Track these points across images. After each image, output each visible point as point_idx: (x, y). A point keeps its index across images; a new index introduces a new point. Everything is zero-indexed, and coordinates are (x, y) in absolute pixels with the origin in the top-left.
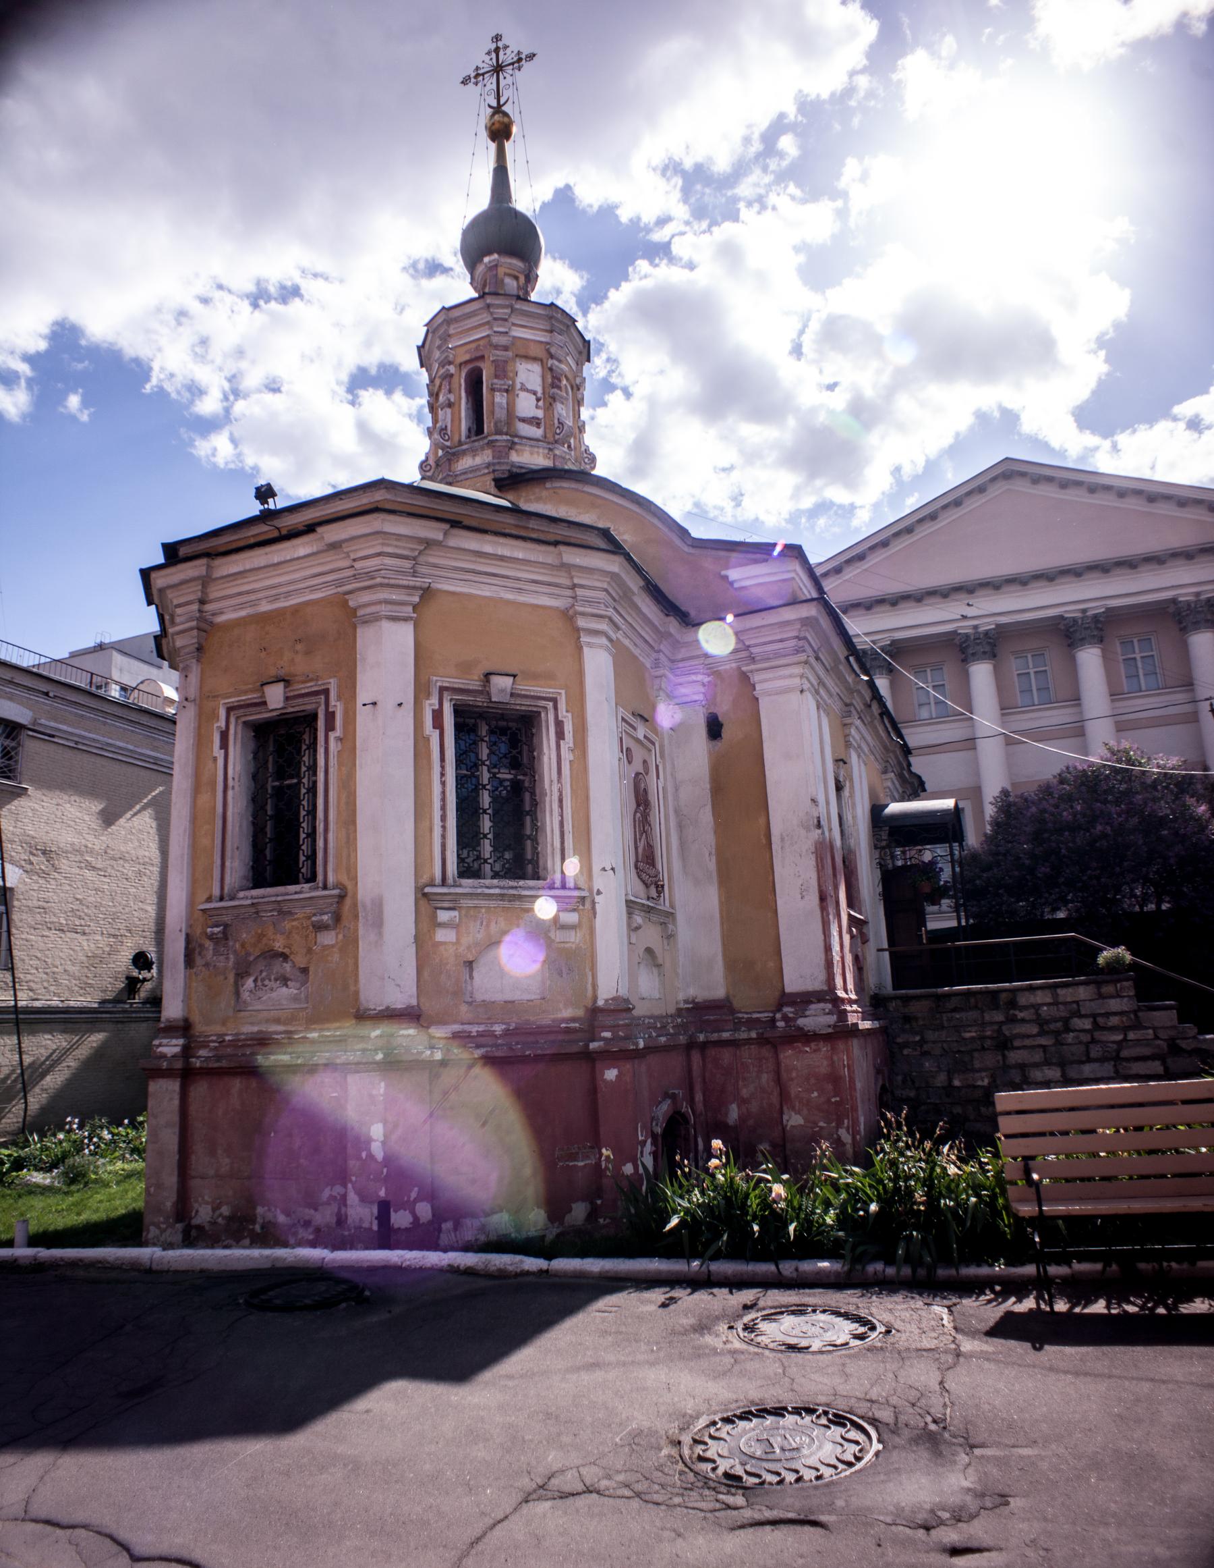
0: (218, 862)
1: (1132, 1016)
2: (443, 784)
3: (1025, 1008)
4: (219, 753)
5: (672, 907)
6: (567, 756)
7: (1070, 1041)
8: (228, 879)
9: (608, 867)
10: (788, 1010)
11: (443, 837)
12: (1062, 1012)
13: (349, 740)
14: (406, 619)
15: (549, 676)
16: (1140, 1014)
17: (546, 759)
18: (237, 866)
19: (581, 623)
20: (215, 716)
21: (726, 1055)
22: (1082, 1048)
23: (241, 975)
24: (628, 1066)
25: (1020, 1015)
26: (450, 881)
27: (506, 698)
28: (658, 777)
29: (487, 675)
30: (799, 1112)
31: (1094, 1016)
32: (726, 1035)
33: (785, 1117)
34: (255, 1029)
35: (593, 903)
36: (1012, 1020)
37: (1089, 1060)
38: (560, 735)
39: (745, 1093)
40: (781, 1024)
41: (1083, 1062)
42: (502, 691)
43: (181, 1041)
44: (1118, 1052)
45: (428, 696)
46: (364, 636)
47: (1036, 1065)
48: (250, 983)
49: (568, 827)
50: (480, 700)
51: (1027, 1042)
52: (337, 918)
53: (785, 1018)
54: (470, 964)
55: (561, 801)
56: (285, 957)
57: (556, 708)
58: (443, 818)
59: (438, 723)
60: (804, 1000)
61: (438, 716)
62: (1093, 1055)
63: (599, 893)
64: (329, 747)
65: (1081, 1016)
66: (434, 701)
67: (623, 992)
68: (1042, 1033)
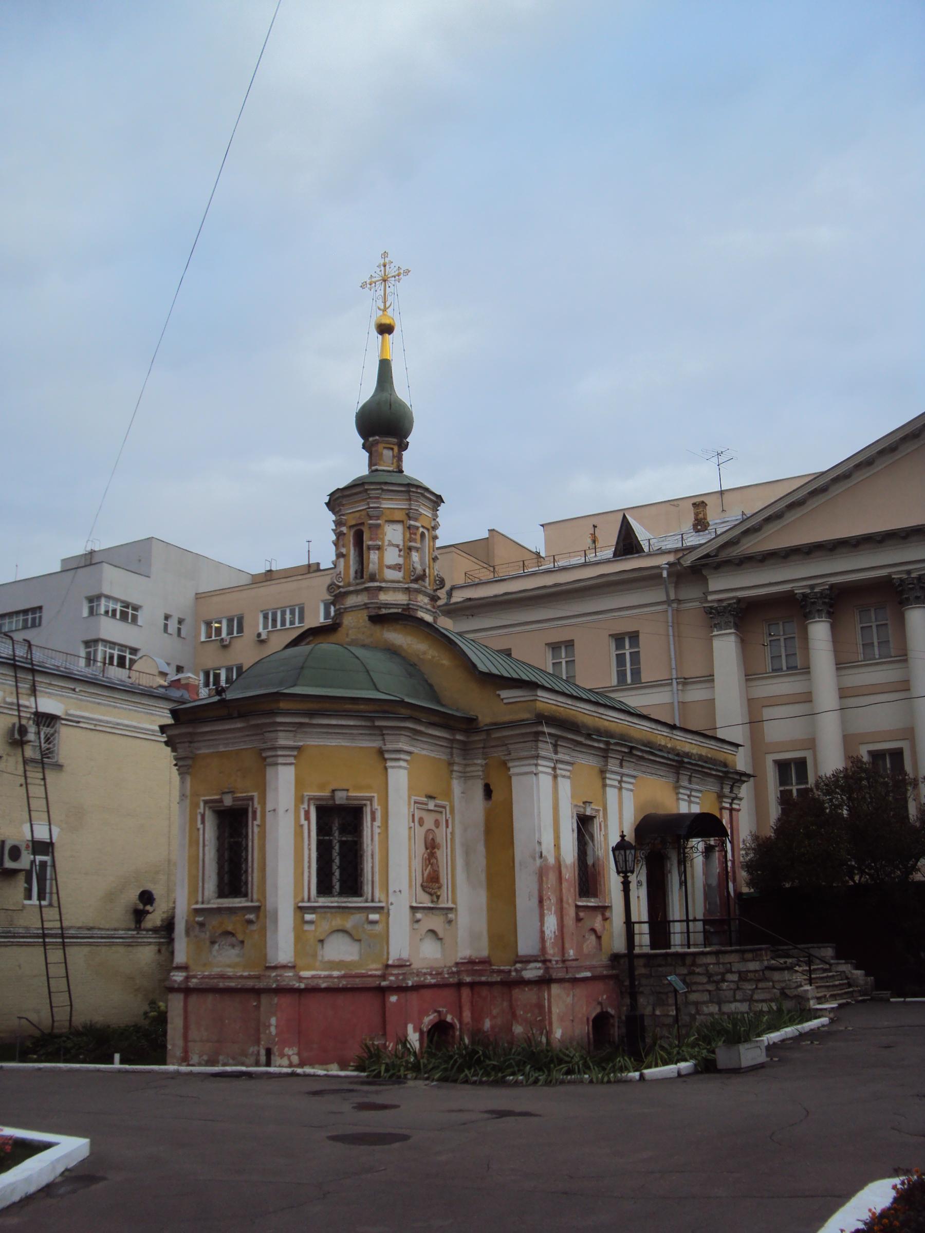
0: (201, 884)
1: (761, 973)
2: (310, 850)
3: (700, 965)
4: (200, 826)
5: (454, 902)
6: (377, 831)
7: (724, 987)
8: (206, 893)
9: (397, 890)
10: (518, 966)
11: (309, 877)
12: (721, 969)
13: (262, 826)
14: (291, 764)
15: (369, 788)
16: (766, 972)
17: (365, 833)
18: (211, 885)
19: (387, 756)
20: (198, 806)
21: (484, 992)
22: (732, 992)
23: (213, 943)
24: (403, 995)
25: (697, 970)
26: (312, 899)
27: (344, 802)
28: (447, 827)
29: (333, 791)
30: (521, 1025)
31: (740, 973)
32: (483, 979)
33: (514, 1028)
34: (219, 970)
35: (388, 910)
36: (692, 973)
37: (736, 1001)
38: (373, 819)
39: (495, 1012)
40: (514, 974)
41: (731, 1002)
42: (341, 798)
43: (184, 974)
44: (752, 996)
45: (303, 803)
46: (270, 771)
47: (704, 1003)
48: (216, 947)
49: (377, 869)
50: (331, 802)
51: (700, 988)
52: (258, 917)
53: (516, 970)
54: (322, 941)
55: (372, 855)
56: (232, 934)
57: (371, 805)
58: (309, 867)
59: (307, 818)
60: (527, 960)
61: (307, 814)
62: (738, 997)
63: (392, 904)
64: (254, 828)
65: (731, 972)
66: (306, 806)
67: (405, 955)
68: (709, 982)
